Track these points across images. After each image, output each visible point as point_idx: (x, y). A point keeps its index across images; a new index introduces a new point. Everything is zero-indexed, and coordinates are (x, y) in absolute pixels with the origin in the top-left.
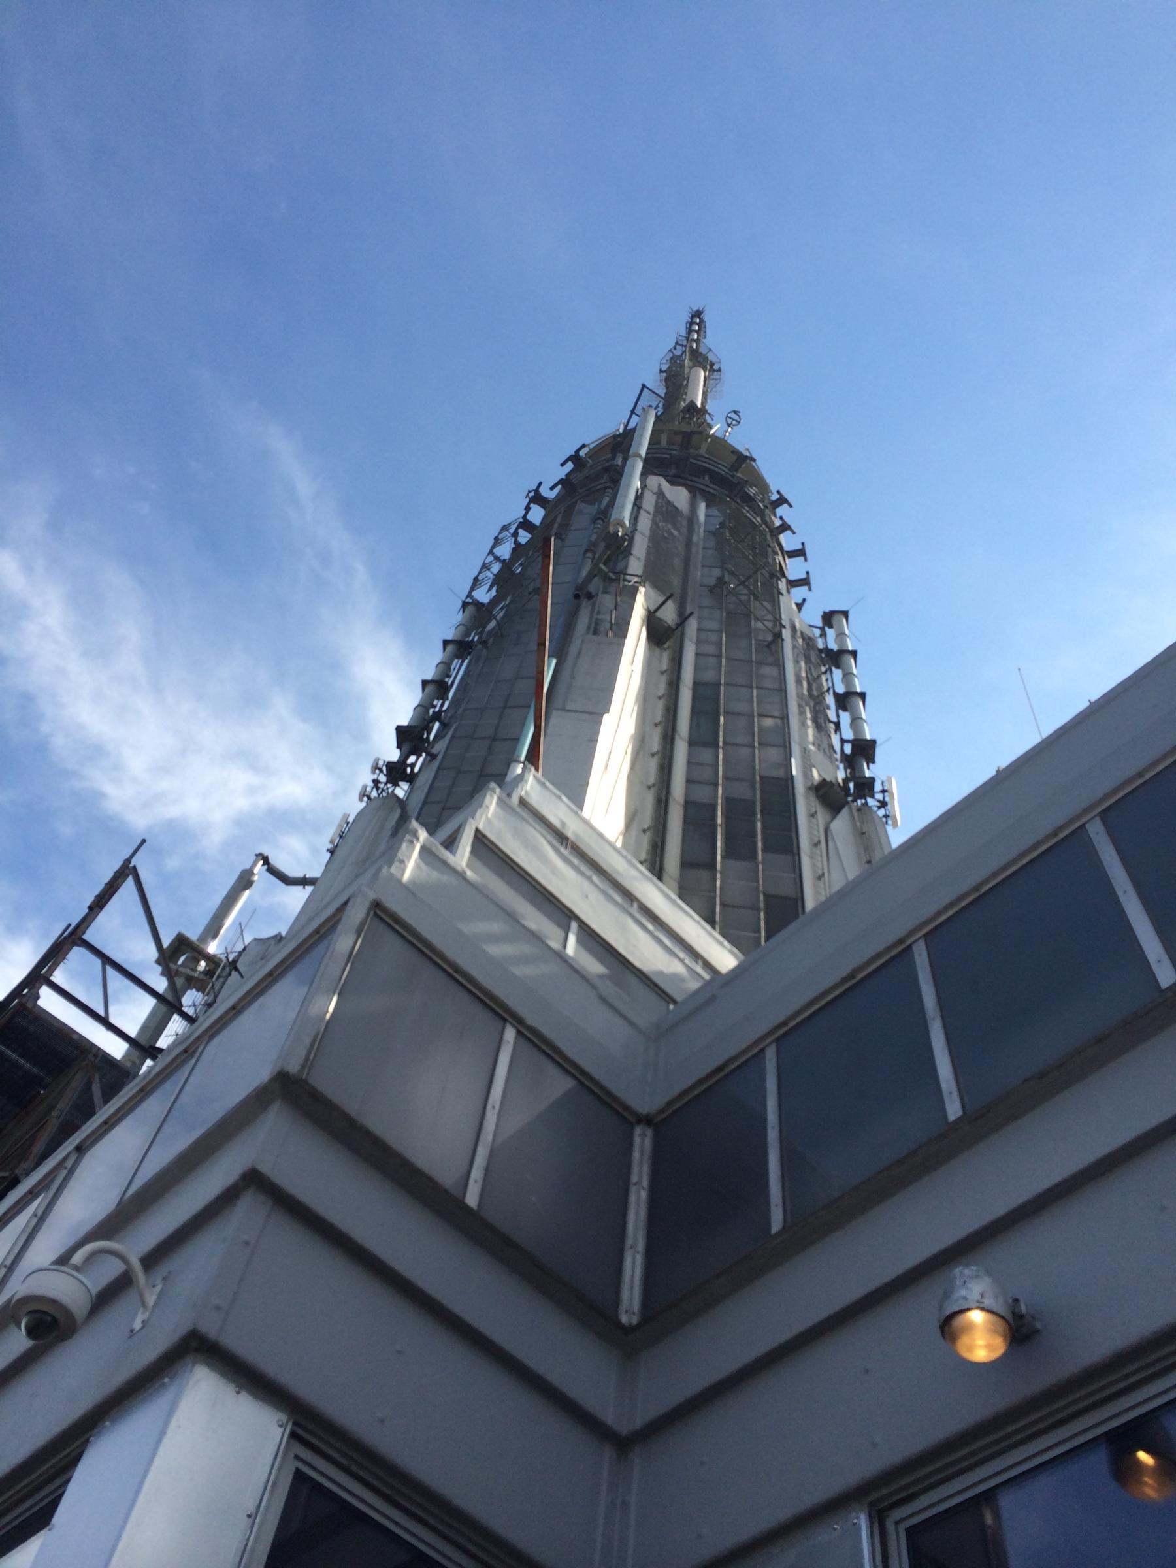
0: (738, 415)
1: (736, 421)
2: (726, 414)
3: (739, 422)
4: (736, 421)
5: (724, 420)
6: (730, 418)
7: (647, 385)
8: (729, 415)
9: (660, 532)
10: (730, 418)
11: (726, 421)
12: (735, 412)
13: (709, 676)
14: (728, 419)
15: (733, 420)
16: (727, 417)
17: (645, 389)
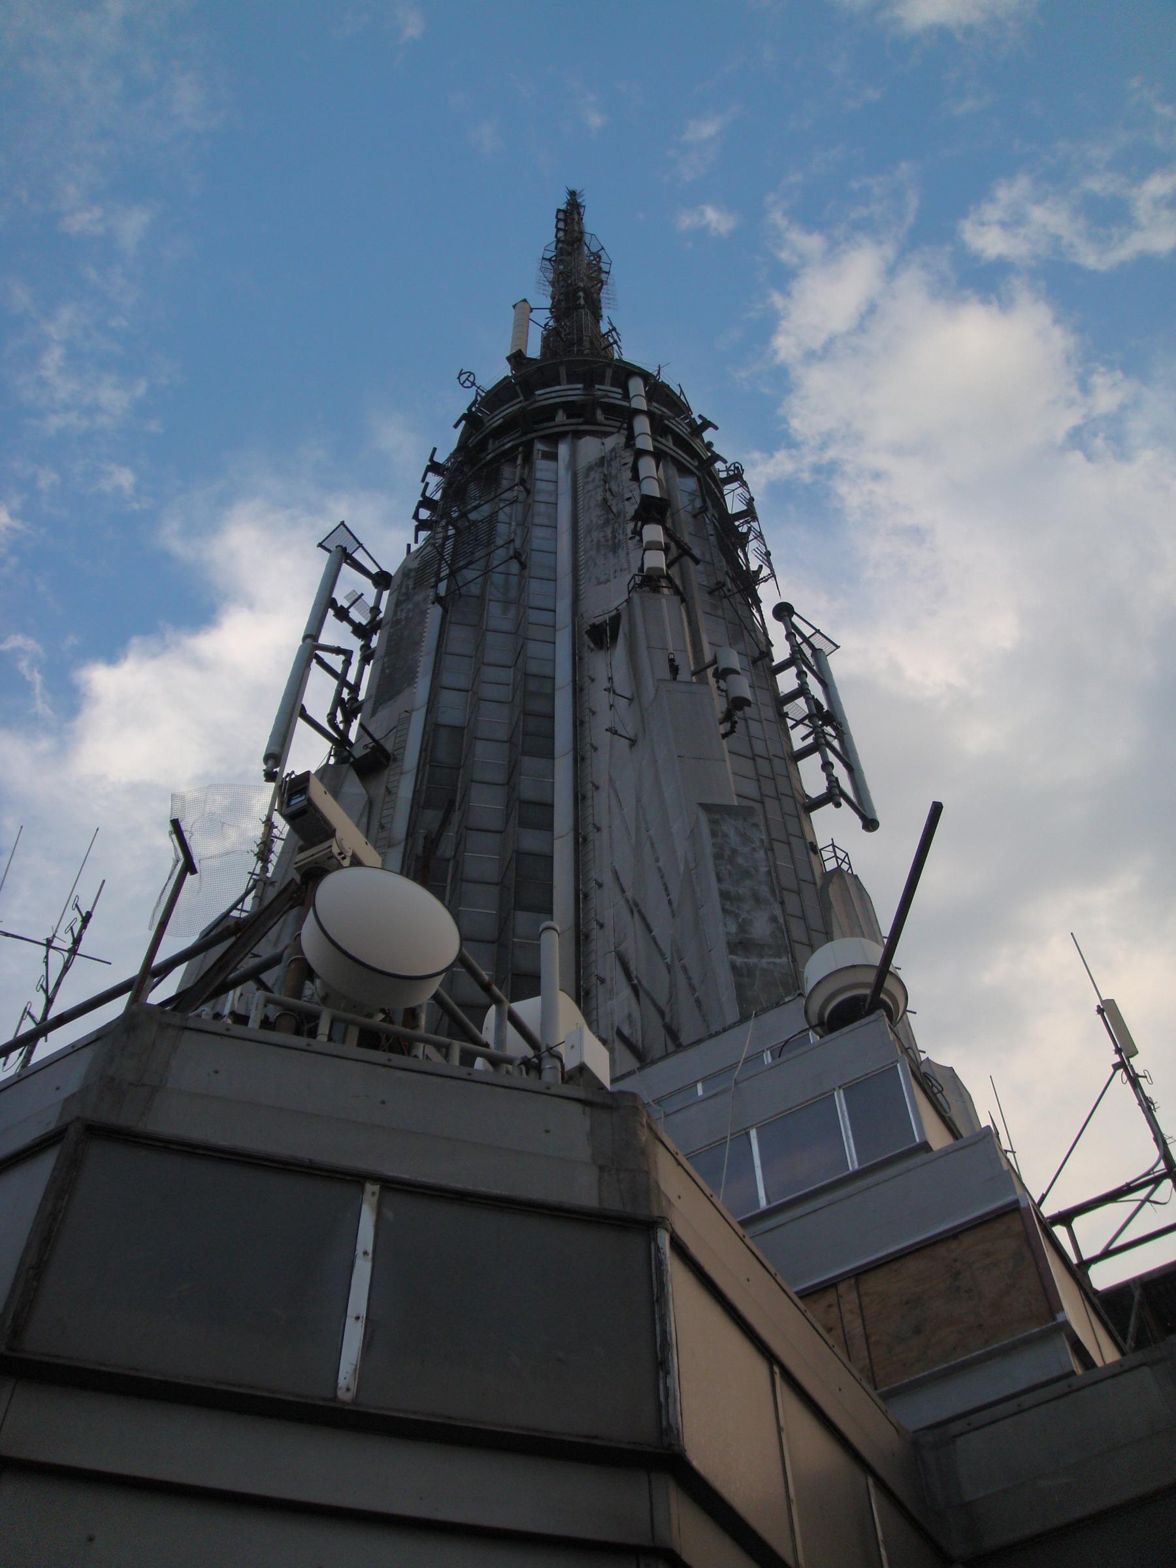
0: (465, 373)
1: (469, 376)
2: (460, 385)
3: (471, 373)
4: (469, 376)
5: (463, 388)
6: (464, 382)
7: (320, 542)
8: (462, 382)
9: (403, 623)
10: (464, 382)
11: (468, 387)
12: (461, 374)
13: (453, 711)
14: (465, 385)
15: (467, 379)
16: (462, 384)
17: (323, 544)
